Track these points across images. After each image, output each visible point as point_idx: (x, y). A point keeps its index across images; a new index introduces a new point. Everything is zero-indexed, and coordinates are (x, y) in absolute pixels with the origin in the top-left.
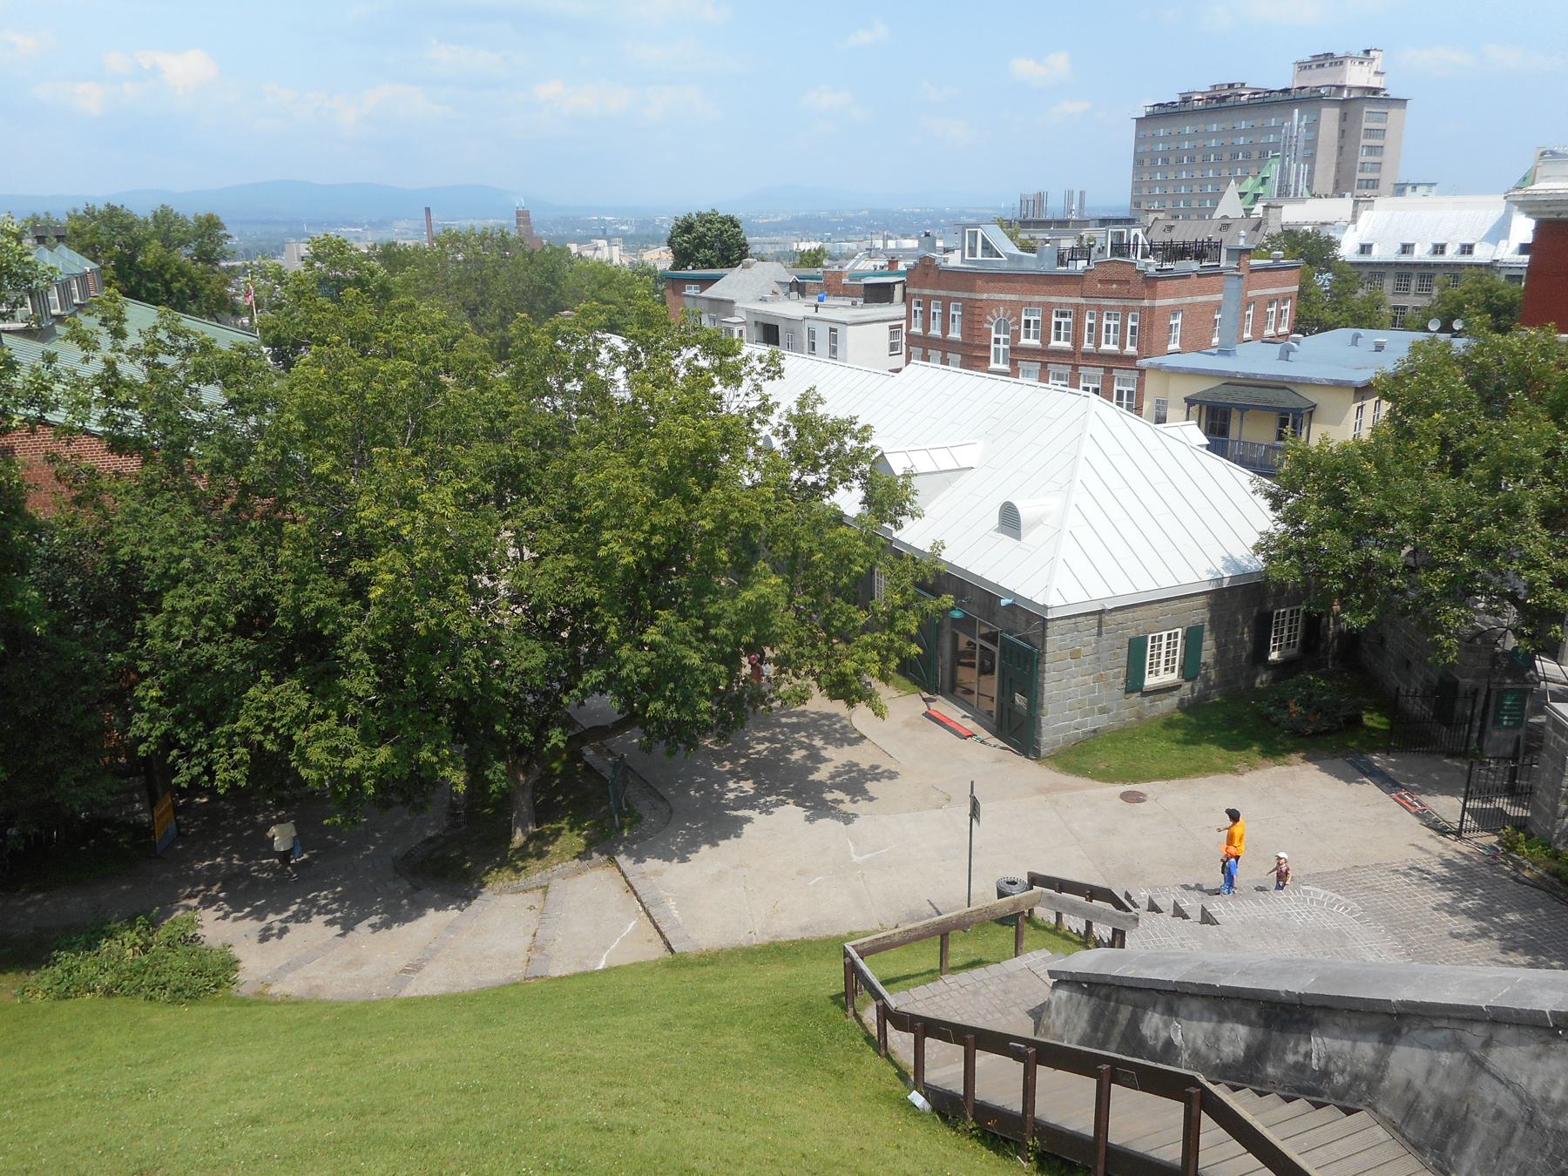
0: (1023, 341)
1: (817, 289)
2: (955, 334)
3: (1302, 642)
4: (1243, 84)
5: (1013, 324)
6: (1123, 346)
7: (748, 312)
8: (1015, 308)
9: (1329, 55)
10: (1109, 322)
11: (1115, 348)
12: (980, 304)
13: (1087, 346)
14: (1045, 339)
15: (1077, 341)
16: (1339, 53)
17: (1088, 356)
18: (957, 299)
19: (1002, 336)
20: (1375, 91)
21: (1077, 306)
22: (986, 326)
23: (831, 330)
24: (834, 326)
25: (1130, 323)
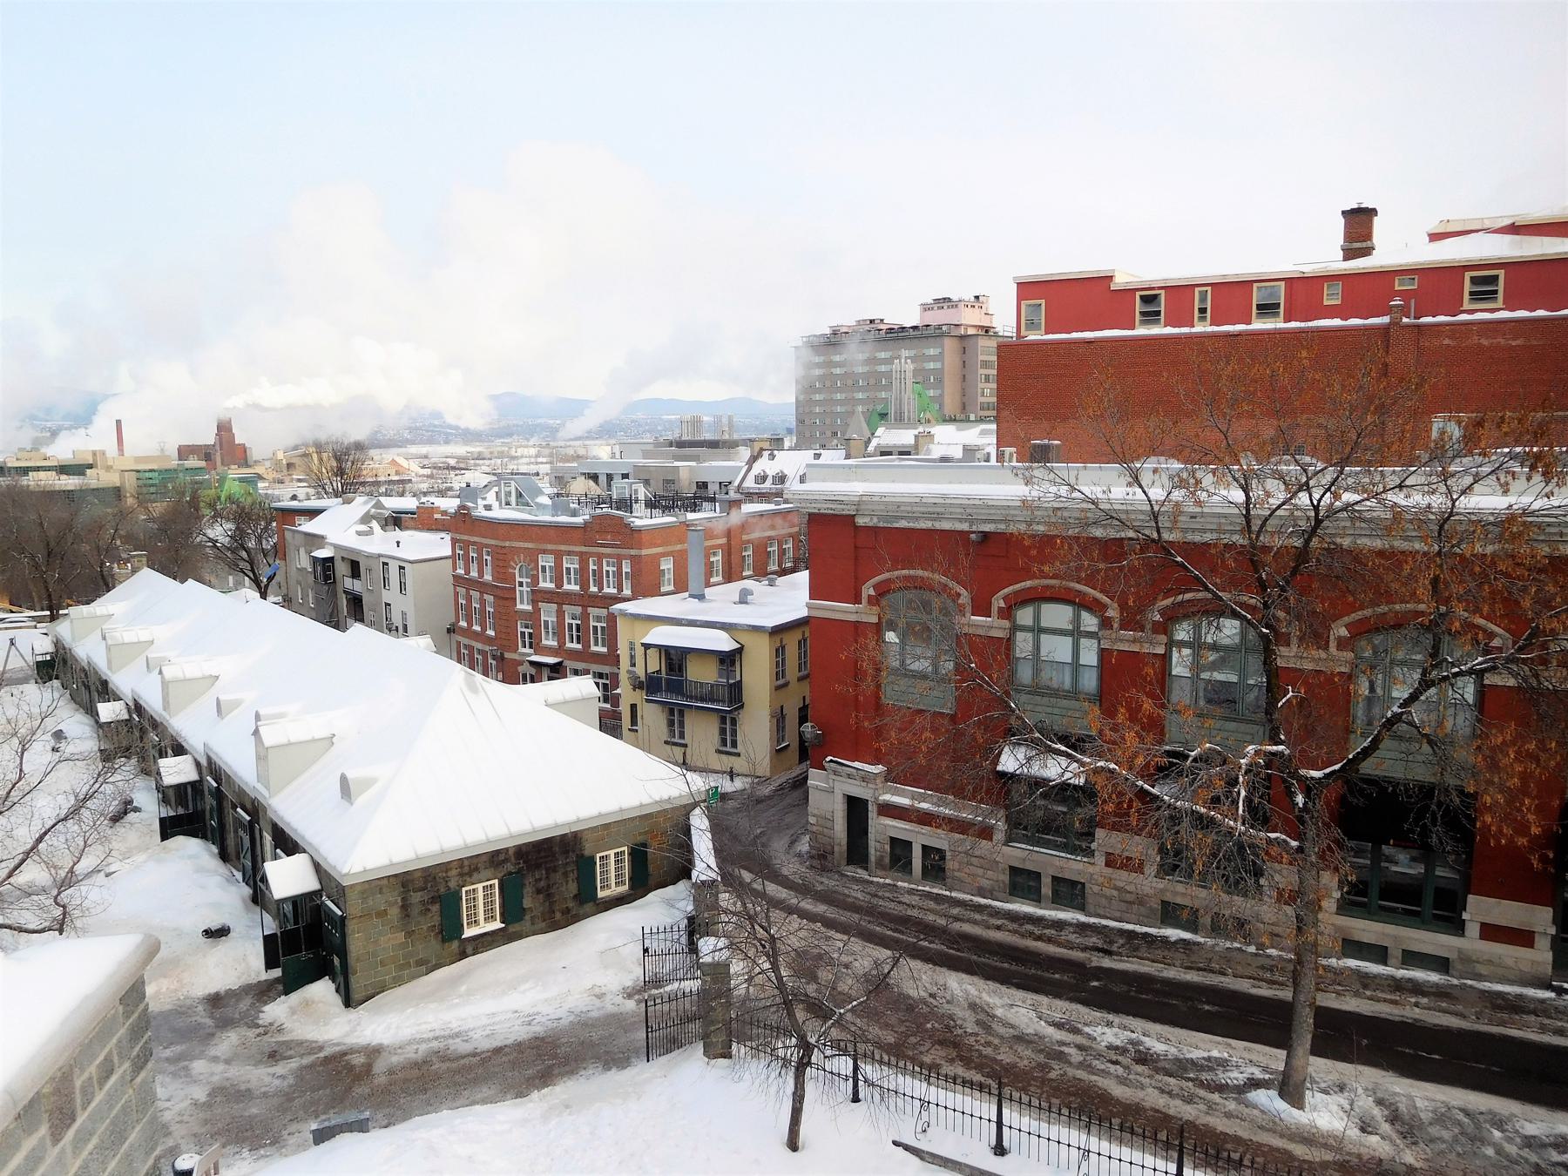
0: (542, 585)
1: (412, 523)
2: (488, 577)
3: (630, 879)
4: (882, 320)
5: (532, 569)
6: (620, 589)
7: (336, 547)
8: (533, 557)
9: (949, 300)
10: (608, 568)
11: (615, 591)
12: (505, 551)
13: (593, 589)
14: (559, 583)
15: (584, 585)
16: (955, 298)
17: (594, 596)
18: (487, 546)
19: (524, 580)
20: (987, 330)
21: (581, 554)
22: (511, 570)
23: (401, 568)
24: (403, 564)
25: (624, 570)
